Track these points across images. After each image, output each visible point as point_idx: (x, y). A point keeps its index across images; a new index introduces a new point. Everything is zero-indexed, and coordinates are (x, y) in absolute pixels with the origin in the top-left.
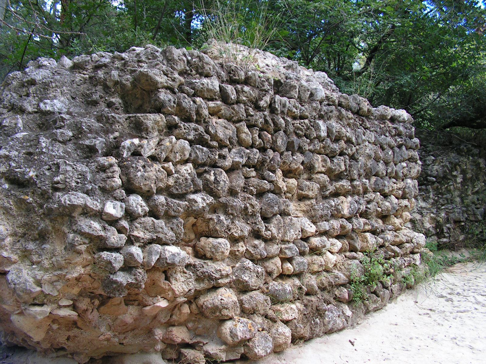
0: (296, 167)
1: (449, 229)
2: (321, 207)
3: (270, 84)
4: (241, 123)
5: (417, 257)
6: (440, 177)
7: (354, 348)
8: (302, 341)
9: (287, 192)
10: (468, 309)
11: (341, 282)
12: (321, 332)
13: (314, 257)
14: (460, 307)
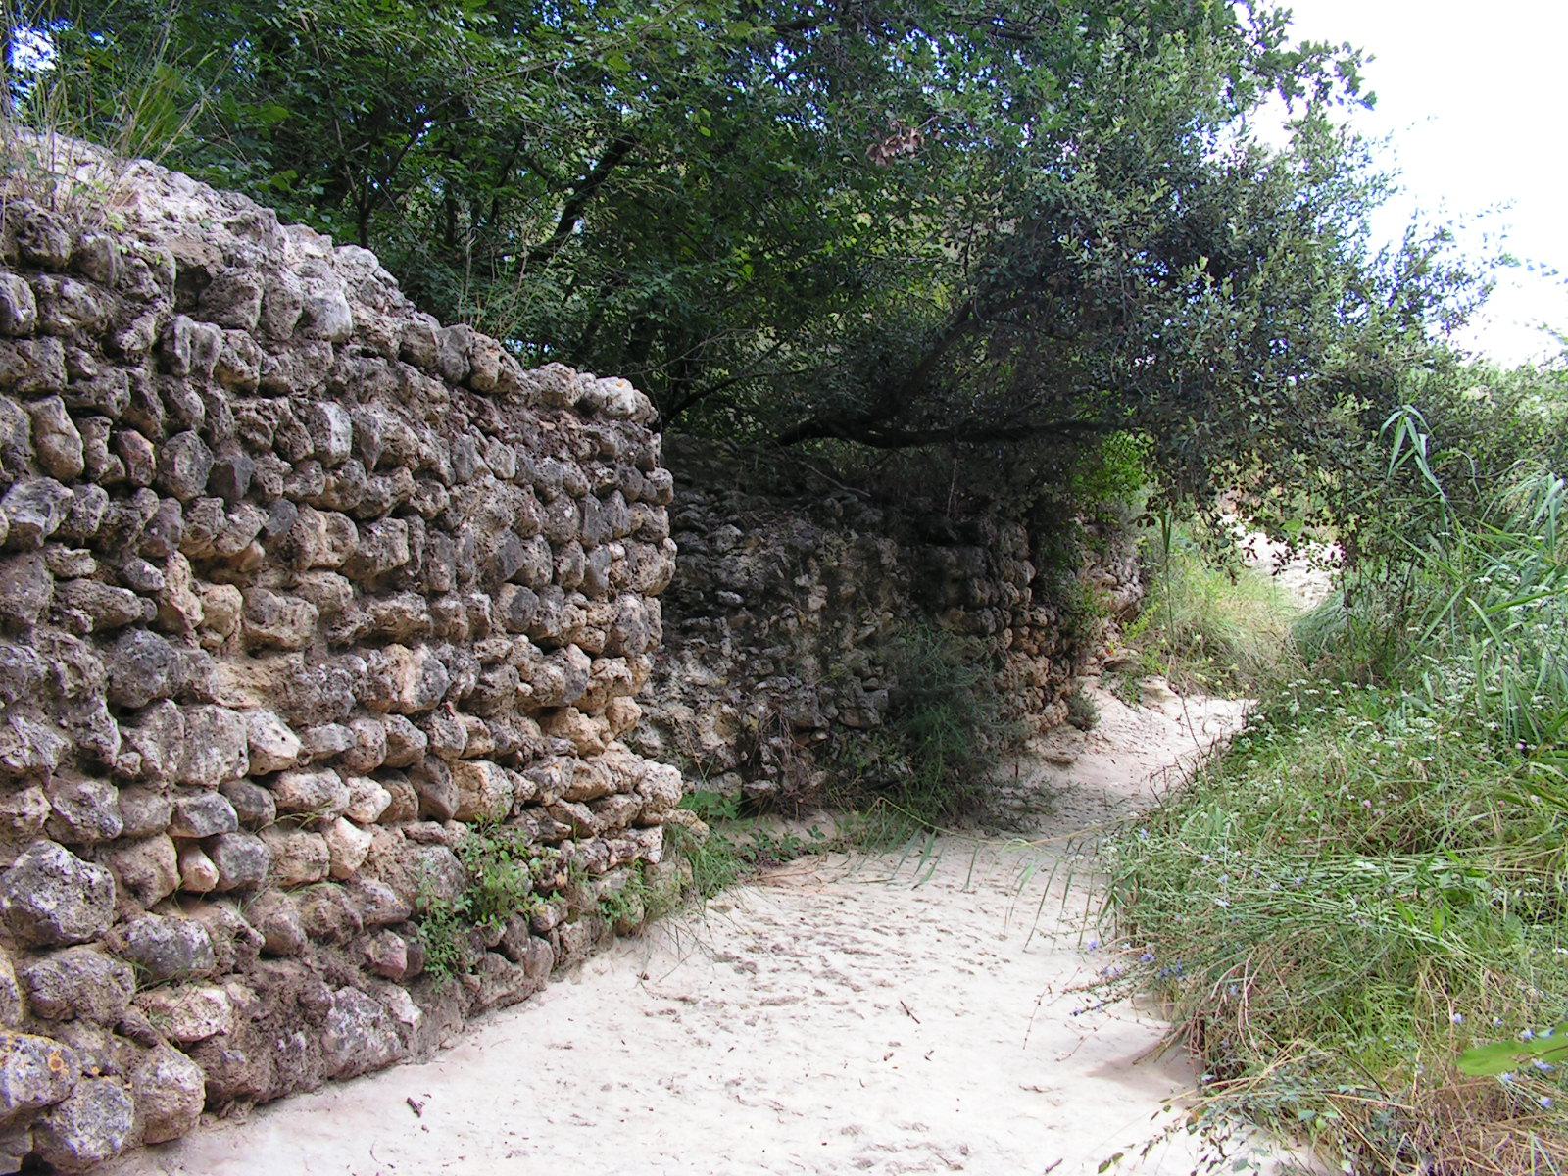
0: (237, 548)
1: (778, 751)
2: (323, 678)
3: (162, 278)
4: (49, 402)
5: (654, 837)
6: (757, 593)
7: (420, 1122)
8: (244, 1107)
9: (210, 627)
10: (797, 993)
11: (385, 914)
12: (314, 1074)
13: (292, 836)
14: (774, 988)
